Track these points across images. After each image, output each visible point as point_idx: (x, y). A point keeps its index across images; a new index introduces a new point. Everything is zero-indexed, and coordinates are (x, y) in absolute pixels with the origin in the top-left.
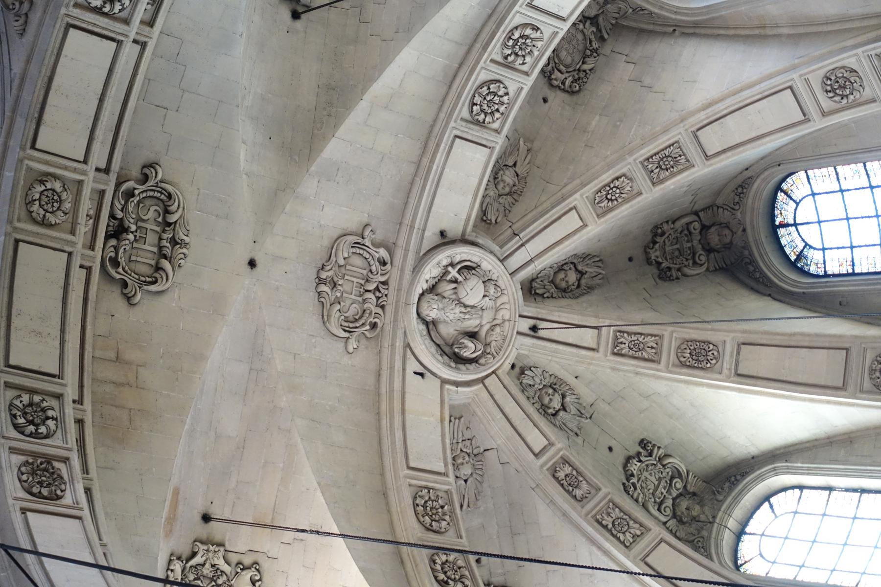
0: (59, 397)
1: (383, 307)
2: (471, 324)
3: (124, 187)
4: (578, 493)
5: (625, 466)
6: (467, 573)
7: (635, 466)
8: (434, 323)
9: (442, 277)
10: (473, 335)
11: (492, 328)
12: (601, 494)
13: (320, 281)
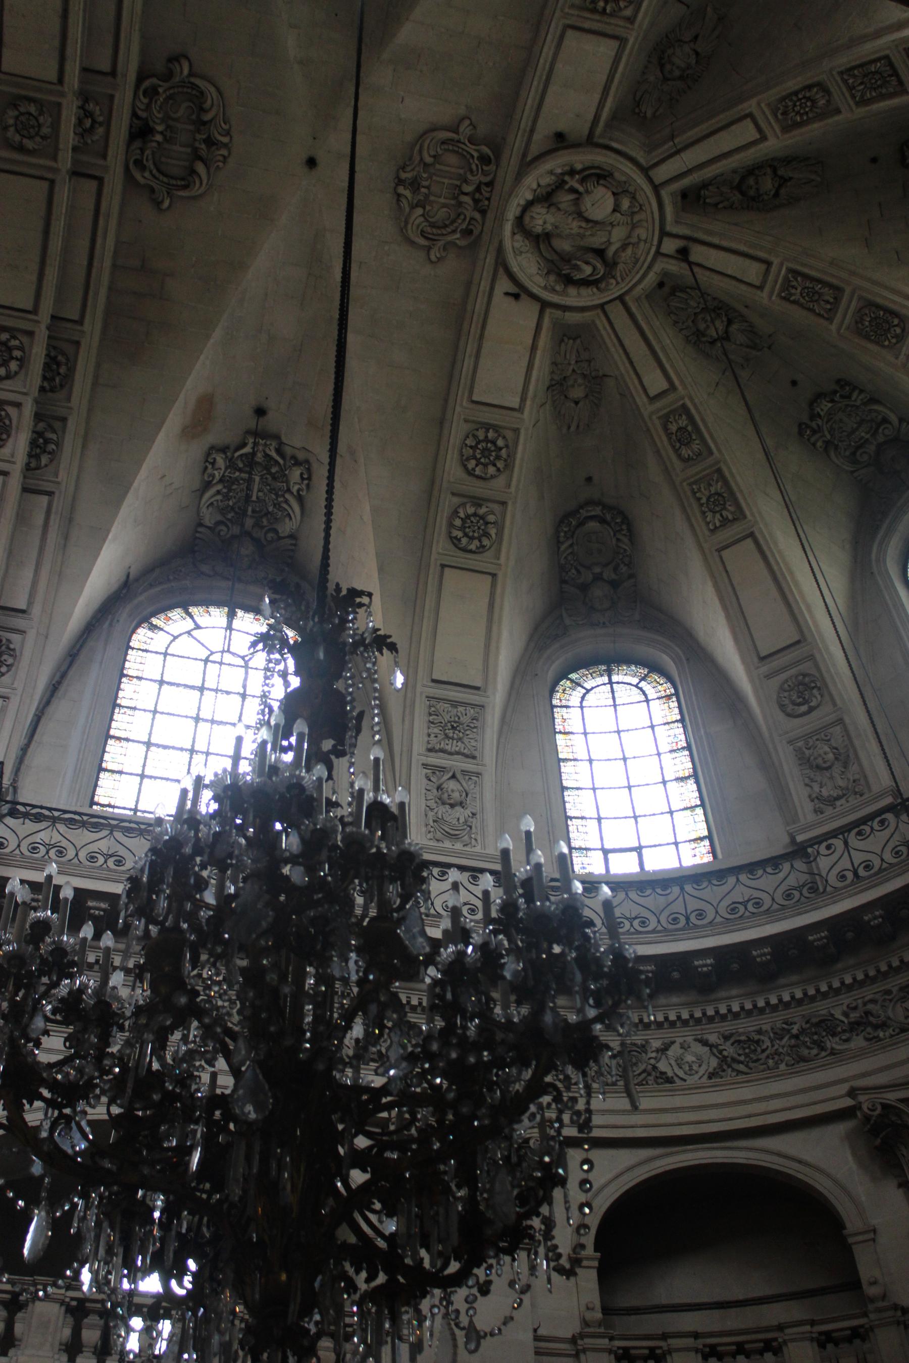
0: (31, 334)
1: (483, 212)
2: (597, 241)
3: (146, 84)
4: (685, 452)
5: (811, 404)
6: (493, 532)
7: (825, 406)
8: (547, 236)
9: (560, 185)
10: (600, 253)
11: (624, 247)
12: (710, 460)
13: (400, 182)
